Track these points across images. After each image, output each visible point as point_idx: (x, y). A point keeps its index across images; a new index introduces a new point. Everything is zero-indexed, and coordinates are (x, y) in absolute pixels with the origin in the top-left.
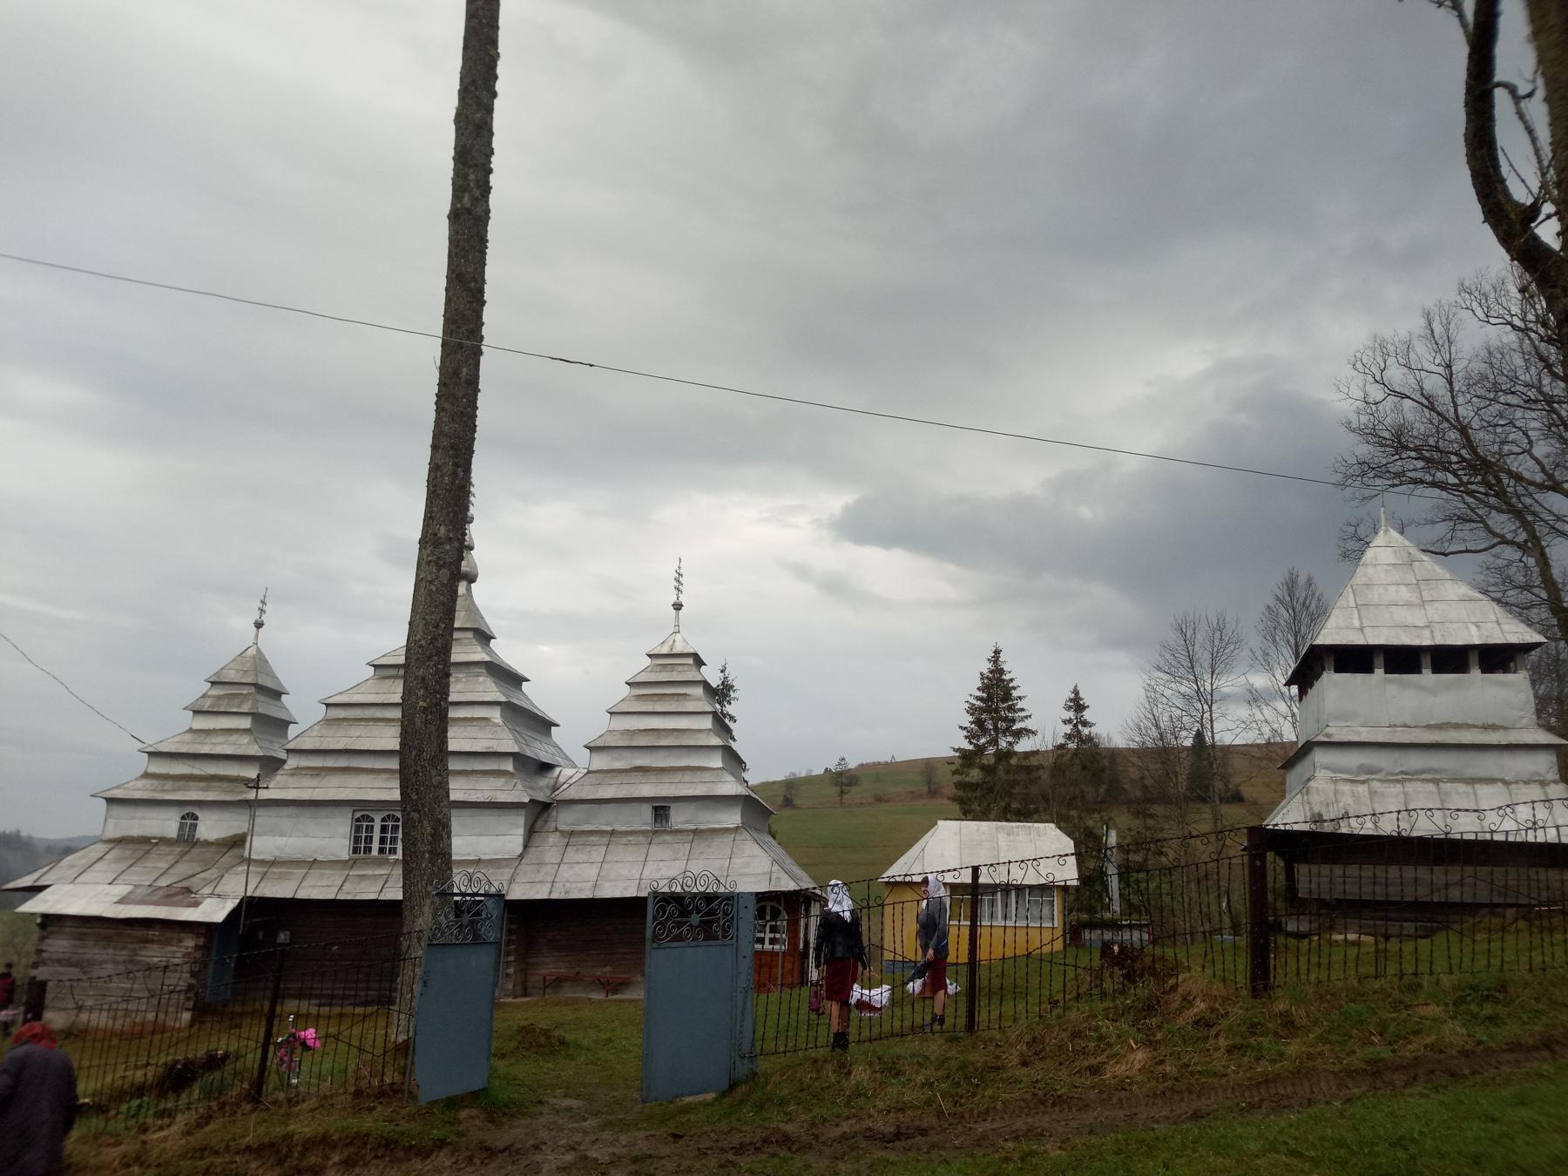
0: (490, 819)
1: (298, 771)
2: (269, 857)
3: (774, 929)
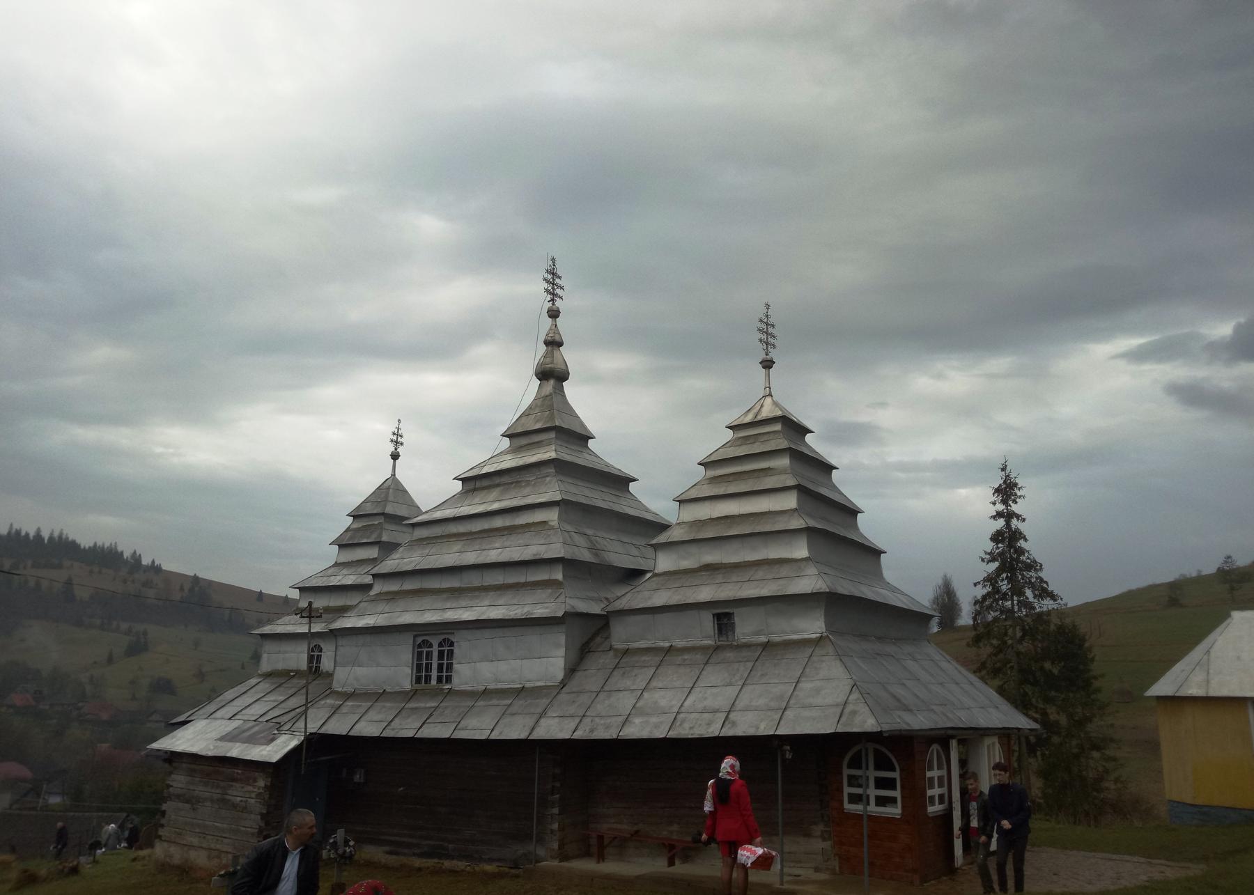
0: (533, 639)
1: (382, 597)
2: (349, 689)
3: (882, 783)
